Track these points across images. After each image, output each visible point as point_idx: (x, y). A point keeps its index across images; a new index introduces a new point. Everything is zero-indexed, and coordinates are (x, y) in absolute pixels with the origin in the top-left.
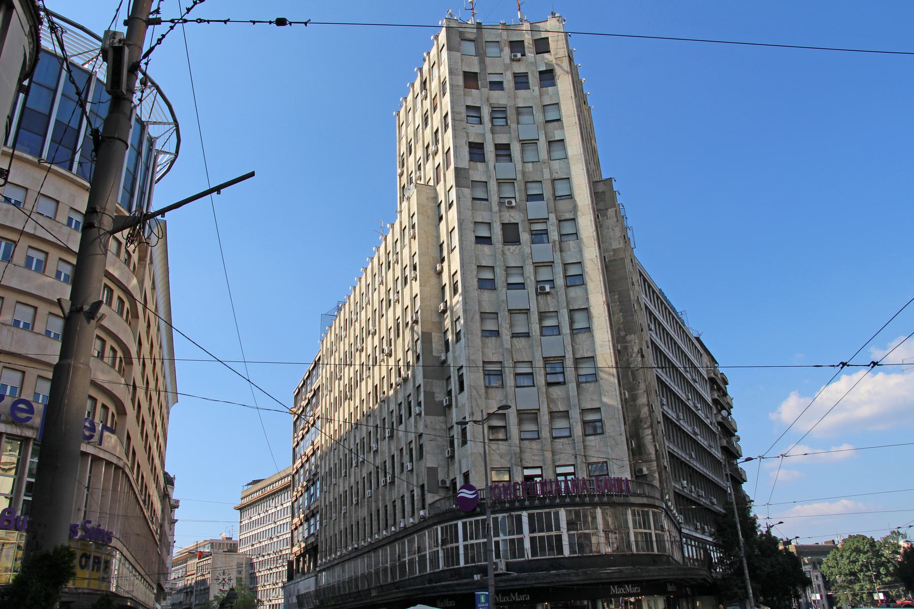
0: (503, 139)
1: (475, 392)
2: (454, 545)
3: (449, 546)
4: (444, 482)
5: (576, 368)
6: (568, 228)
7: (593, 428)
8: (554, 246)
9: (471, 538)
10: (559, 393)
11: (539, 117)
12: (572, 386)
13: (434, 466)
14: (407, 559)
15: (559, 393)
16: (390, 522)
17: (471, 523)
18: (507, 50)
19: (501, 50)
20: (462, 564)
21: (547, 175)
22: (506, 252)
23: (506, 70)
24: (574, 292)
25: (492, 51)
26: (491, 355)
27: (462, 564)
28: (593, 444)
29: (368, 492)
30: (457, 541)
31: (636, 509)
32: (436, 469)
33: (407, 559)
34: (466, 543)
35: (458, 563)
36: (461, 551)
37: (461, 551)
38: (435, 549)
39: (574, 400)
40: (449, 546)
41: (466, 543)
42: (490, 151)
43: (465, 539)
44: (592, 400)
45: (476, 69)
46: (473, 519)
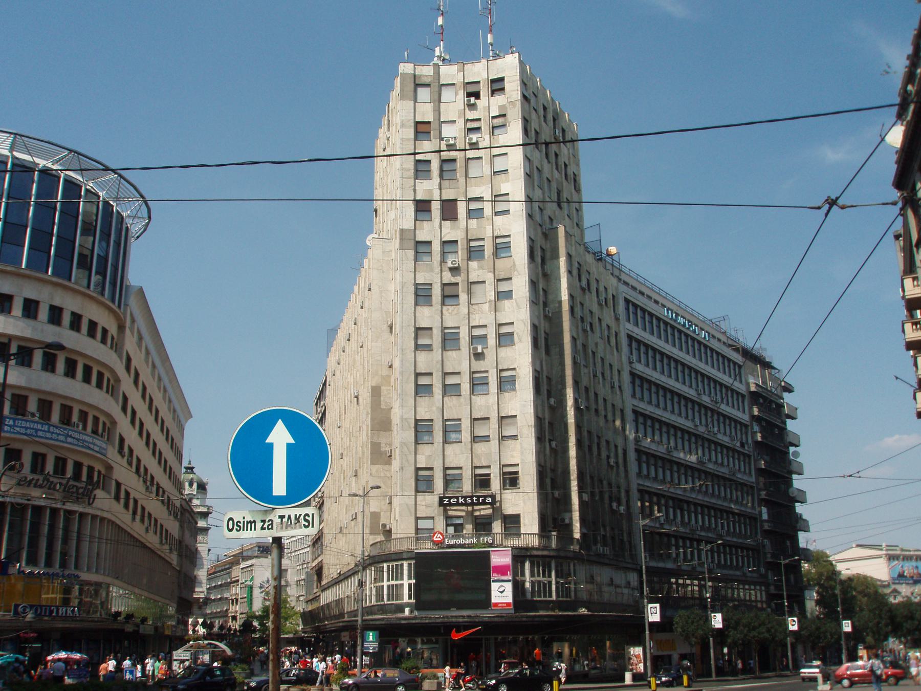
0: (448, 195)
1: (405, 449)
4: (384, 526)
5: (500, 426)
6: (504, 287)
7: (511, 480)
8: (490, 307)
11: (487, 171)
12: (494, 443)
14: (385, 584)
18: (461, 94)
19: (457, 94)
21: (488, 233)
22: (444, 312)
23: (459, 117)
24: (504, 352)
25: (447, 94)
31: (536, 560)
32: (379, 513)
40: (378, 584)
42: (436, 207)
43: (388, 580)
44: (512, 456)
45: (429, 117)
46: (394, 563)
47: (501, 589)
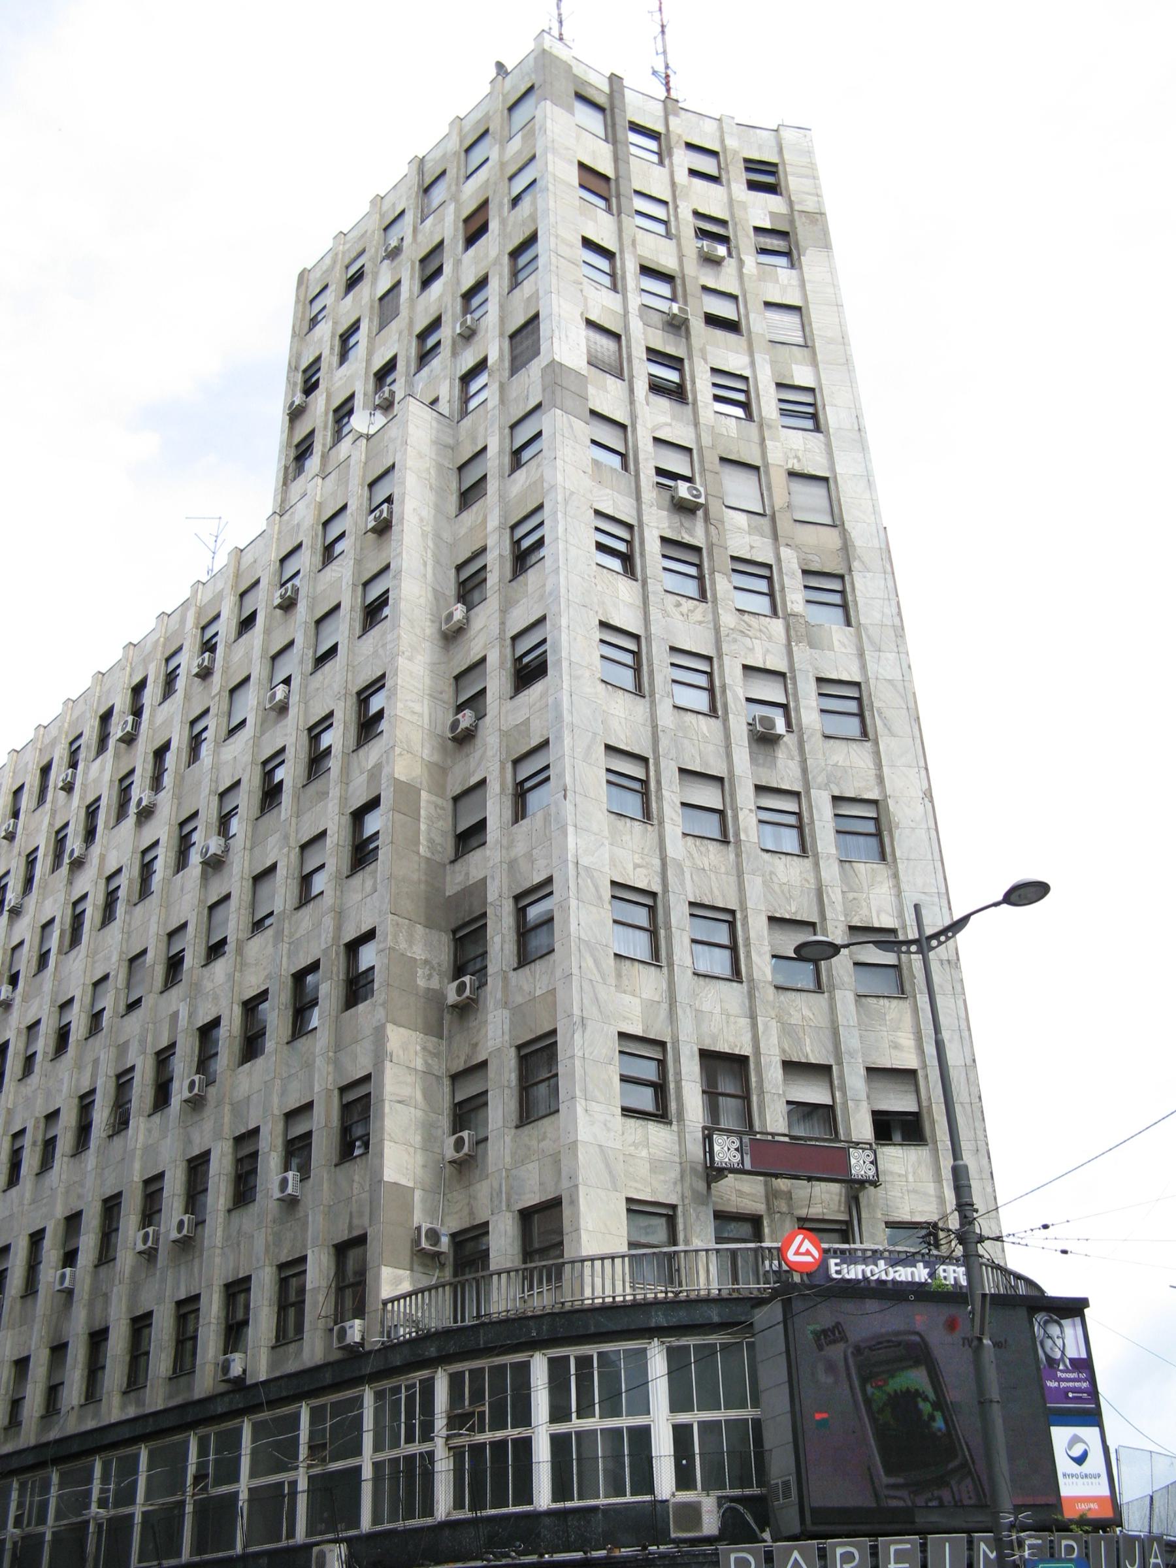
2: (511, 1433)
3: (487, 1437)
4: (434, 1236)
9: (585, 1411)
10: (806, 1012)
13: (403, 1181)
15: (806, 1012)
16: (161, 1362)
17: (584, 1363)
20: (543, 1497)
26: (630, 867)
27: (543, 1497)
28: (897, 1168)
29: (50, 1272)
30: (524, 1417)
33: (244, 1486)
34: (561, 1428)
35: (525, 1493)
36: (542, 1452)
37: (542, 1452)
38: (416, 1448)
39: (850, 1040)
41: (561, 1428)
43: (558, 1413)
46: (592, 1350)
47: (1077, 1451)
